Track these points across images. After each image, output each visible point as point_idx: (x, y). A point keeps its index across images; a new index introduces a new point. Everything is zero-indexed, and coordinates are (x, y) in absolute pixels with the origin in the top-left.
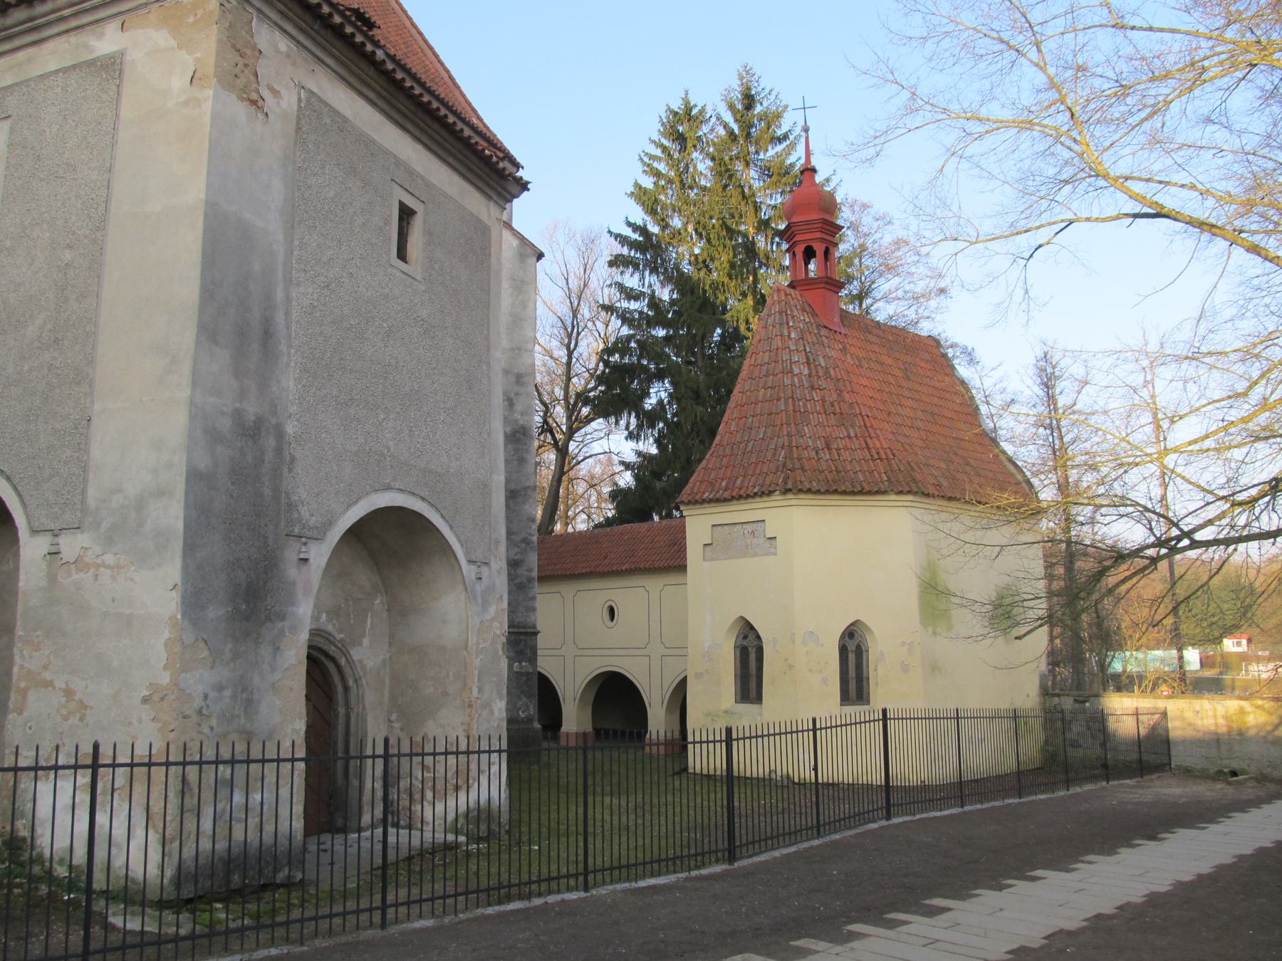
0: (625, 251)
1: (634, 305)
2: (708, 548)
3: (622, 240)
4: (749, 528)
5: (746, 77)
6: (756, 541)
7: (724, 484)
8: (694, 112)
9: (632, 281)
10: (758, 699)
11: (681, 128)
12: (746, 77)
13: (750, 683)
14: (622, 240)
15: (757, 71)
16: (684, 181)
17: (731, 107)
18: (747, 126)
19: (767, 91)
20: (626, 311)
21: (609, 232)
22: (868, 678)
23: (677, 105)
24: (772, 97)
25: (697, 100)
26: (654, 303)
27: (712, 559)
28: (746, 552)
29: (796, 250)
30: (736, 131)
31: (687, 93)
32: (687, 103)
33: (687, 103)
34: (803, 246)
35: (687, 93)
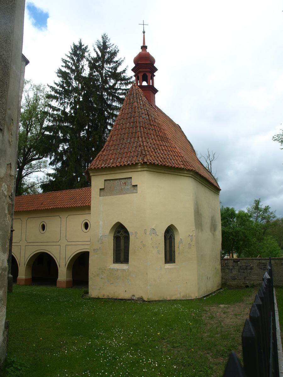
0: (53, 93)
1: (55, 112)
2: (102, 191)
3: (53, 89)
4: (123, 181)
5: (104, 38)
6: (126, 187)
7: (112, 161)
8: (83, 47)
9: (54, 103)
10: (126, 260)
11: (78, 51)
12: (104, 38)
13: (122, 253)
14: (53, 89)
15: (109, 37)
16: (78, 71)
17: (99, 48)
18: (103, 55)
19: (112, 44)
20: (53, 114)
21: (48, 85)
22: (174, 252)
23: (77, 44)
24: (114, 47)
25: (85, 44)
26: (64, 112)
27: (104, 196)
28: (121, 192)
29: (139, 75)
30: (100, 55)
31: (81, 41)
32: (80, 43)
33: (80, 43)
34: (142, 74)
35: (81, 41)
